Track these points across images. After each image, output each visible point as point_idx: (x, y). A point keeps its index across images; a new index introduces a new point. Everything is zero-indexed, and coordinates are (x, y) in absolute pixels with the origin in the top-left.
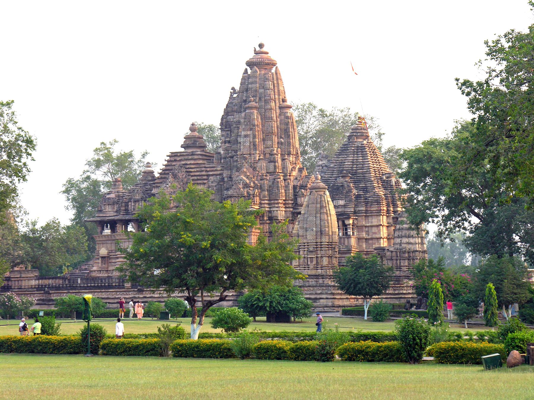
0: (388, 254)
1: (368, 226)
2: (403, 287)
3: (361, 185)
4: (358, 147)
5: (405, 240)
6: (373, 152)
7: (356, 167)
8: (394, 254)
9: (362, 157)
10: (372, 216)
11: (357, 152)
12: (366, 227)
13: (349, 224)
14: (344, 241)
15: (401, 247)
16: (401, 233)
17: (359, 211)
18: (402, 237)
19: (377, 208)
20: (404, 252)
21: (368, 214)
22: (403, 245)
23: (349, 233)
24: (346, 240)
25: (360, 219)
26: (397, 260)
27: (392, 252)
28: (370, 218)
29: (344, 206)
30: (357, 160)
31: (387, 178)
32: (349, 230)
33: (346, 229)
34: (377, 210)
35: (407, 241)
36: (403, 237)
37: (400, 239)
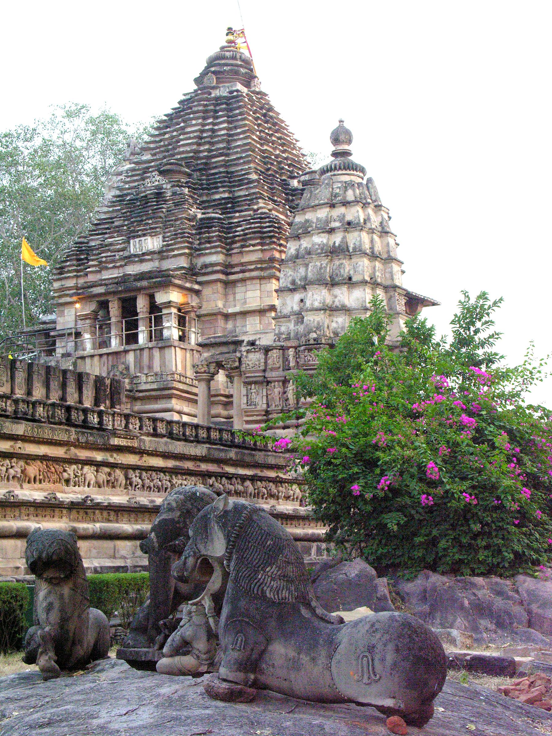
0: (254, 359)
1: (235, 315)
2: (278, 481)
3: (217, 197)
4: (217, 99)
5: (317, 296)
6: (265, 115)
7: (209, 151)
8: (274, 354)
9: (229, 122)
10: (243, 280)
11: (216, 112)
12: (227, 316)
13: (169, 304)
14: (151, 358)
15: (301, 328)
16: (302, 271)
17: (206, 266)
18: (303, 286)
19: (259, 255)
20: (313, 346)
21: (232, 277)
22: (311, 319)
23: (166, 333)
24: (156, 354)
25: (207, 291)
26: (285, 382)
27: (267, 350)
28: (240, 289)
29: (161, 254)
30: (213, 131)
31: (305, 183)
32: (166, 324)
33: (159, 320)
34: (261, 261)
35: (329, 300)
36: (311, 283)
37: (297, 297)
